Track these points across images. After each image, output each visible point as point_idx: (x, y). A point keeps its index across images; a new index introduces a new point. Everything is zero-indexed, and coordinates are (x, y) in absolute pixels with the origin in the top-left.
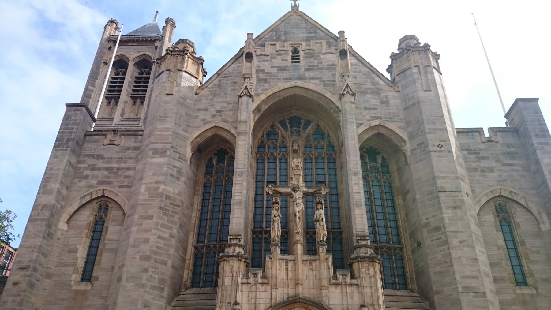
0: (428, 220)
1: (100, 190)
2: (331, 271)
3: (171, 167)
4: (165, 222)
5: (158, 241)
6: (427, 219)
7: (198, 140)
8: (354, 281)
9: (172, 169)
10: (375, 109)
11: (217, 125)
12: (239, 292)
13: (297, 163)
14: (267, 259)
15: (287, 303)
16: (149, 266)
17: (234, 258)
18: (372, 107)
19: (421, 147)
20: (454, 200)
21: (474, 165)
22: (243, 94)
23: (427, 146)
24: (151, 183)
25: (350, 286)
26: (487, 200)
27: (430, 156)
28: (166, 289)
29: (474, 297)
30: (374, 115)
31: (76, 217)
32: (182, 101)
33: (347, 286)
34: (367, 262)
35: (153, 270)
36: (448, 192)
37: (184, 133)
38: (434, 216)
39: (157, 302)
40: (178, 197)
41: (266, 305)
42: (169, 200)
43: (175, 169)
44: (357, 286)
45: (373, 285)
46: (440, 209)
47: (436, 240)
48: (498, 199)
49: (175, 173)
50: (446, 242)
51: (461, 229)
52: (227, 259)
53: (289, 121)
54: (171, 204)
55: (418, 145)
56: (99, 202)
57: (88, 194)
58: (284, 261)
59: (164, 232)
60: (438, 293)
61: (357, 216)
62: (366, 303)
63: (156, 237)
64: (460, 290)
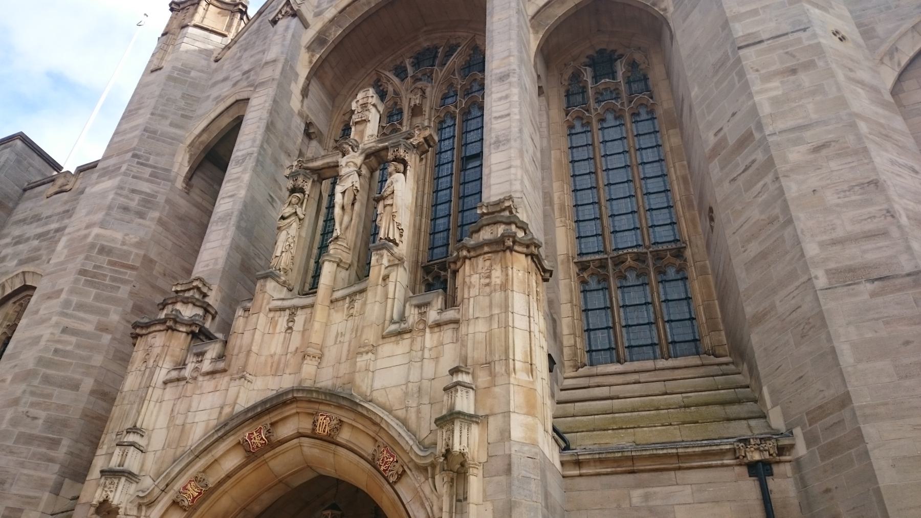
0: (721, 134)
1: (17, 275)
3: (125, 192)
4: (90, 300)
5: (62, 339)
7: (204, 137)
8: (451, 314)
9: (126, 197)
11: (238, 98)
12: (152, 403)
14: (240, 312)
15: (259, 410)
16: (24, 392)
20: (787, 53)
22: (280, 16)
24: (79, 230)
25: (436, 329)
28: (66, 442)
29: (873, 295)
32: (178, 74)
33: (428, 330)
34: (486, 256)
35: (34, 399)
36: (769, 39)
37: (173, 130)
39: (31, 472)
40: (135, 251)
41: (207, 425)
42: (108, 255)
43: (137, 197)
45: (496, 311)
46: (746, 86)
47: (743, 172)
49: (133, 204)
50: (770, 163)
51: (814, 117)
52: (144, 332)
53: (411, 60)
54: (111, 263)
56: (18, 300)
58: (287, 310)
59: (82, 320)
60: (759, 319)
61: (494, 168)
62: (469, 362)
63: (57, 331)
64: (821, 281)
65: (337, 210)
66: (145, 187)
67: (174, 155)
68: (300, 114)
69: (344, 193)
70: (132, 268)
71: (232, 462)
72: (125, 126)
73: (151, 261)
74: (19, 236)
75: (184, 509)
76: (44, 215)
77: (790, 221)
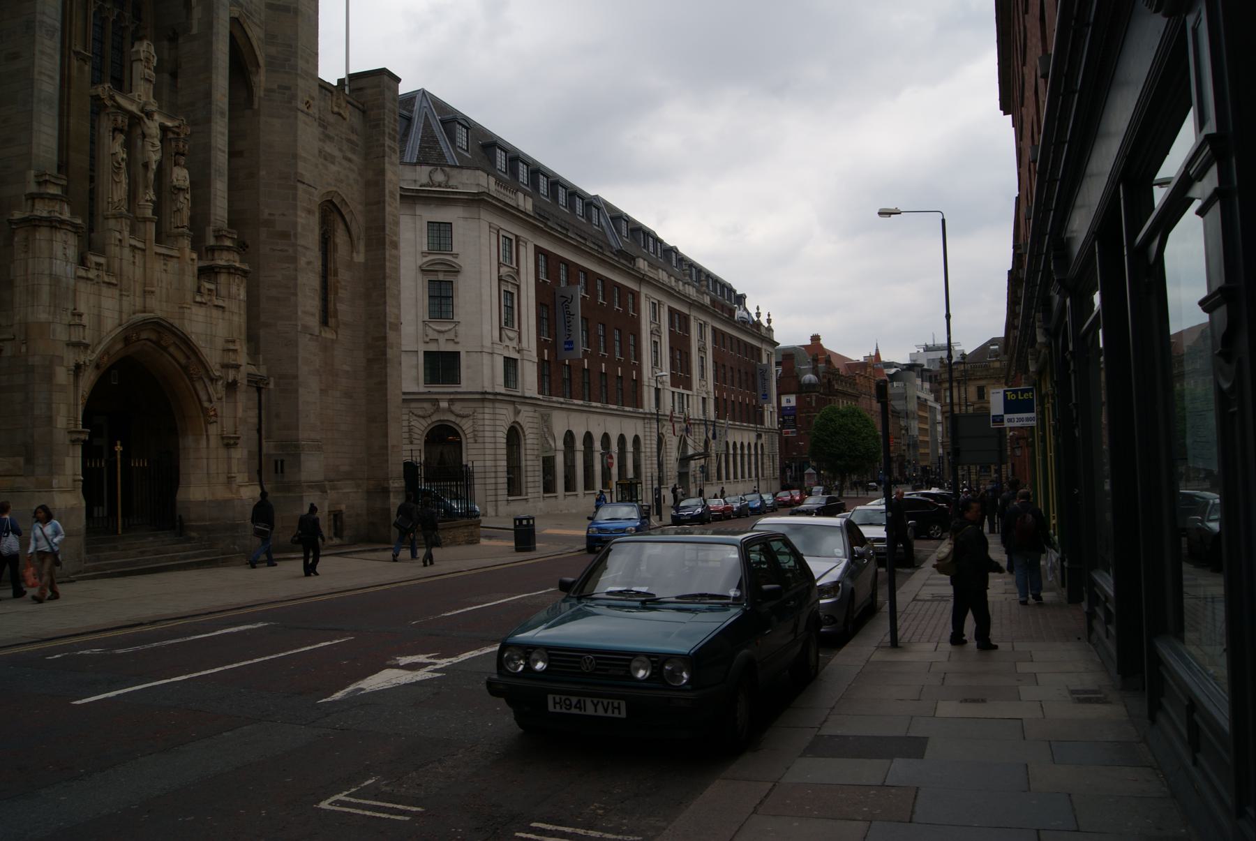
2: (196, 279)
6: (270, 214)
13: (148, 54)
17: (69, 228)
19: (284, 94)
23: (293, 97)
27: (296, 118)
38: (284, 215)
44: (221, 309)
50: (294, 260)
55: (279, 87)
64: (299, 328)
77: (295, 294)
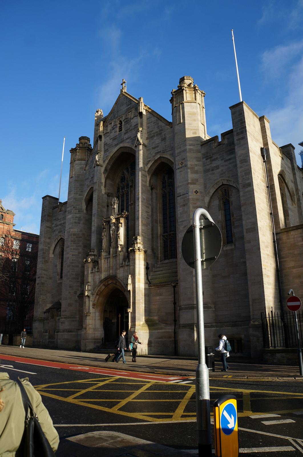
3: (74, 218)
10: (157, 147)
18: (157, 145)
21: (208, 167)
26: (215, 190)
30: (157, 151)
31: (55, 250)
37: (80, 197)
43: (77, 219)
48: (223, 187)
49: (77, 221)
54: (76, 237)
57: (56, 239)
65: (111, 235)
66: (78, 215)
67: (82, 204)
68: (105, 193)
69: (112, 231)
70: (81, 237)
71: (103, 287)
72: (70, 197)
73: (84, 234)
74: (56, 224)
75: (98, 295)
76: (59, 218)
